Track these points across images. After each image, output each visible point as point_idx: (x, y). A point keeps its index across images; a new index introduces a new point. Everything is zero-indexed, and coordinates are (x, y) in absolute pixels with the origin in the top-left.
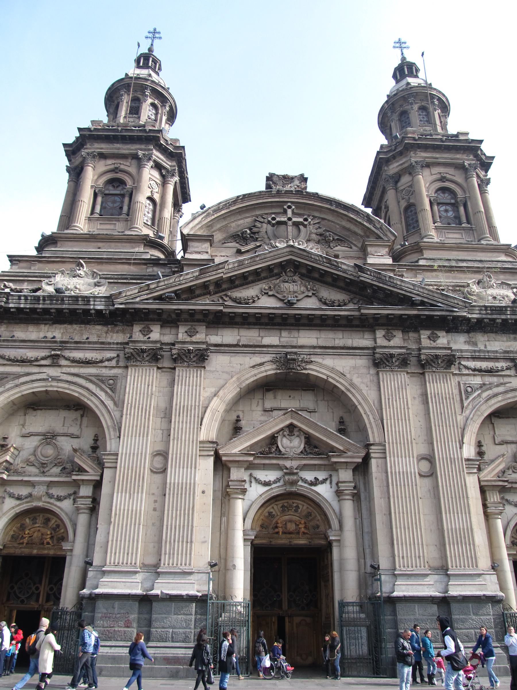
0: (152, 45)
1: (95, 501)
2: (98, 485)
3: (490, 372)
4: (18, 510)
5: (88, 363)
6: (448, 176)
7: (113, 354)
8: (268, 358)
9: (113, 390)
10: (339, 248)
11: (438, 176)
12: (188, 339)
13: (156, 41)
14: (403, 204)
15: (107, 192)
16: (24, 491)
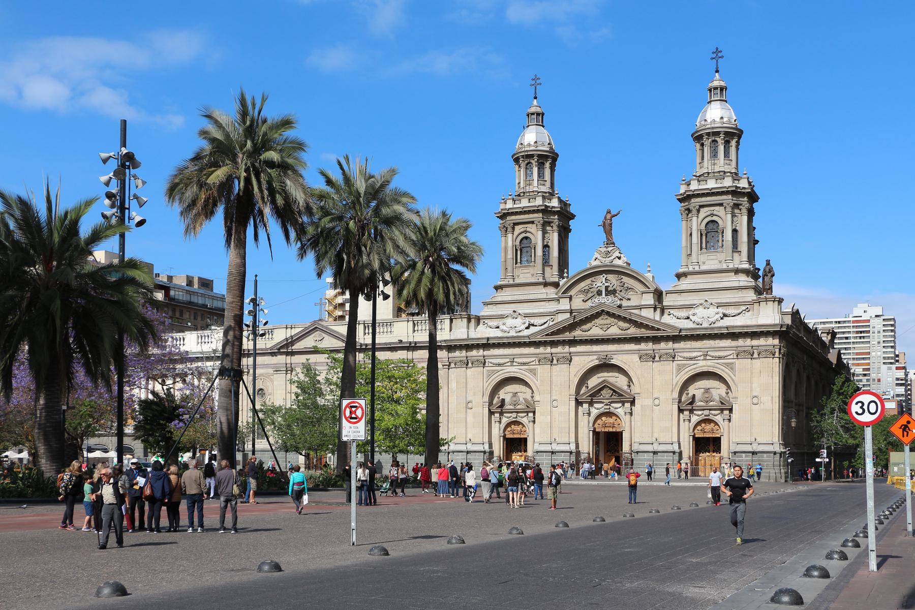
0: (535, 92)
1: (534, 418)
2: (534, 413)
3: (691, 359)
4: (508, 422)
5: (524, 364)
6: (715, 213)
7: (533, 359)
8: (595, 357)
9: (535, 374)
10: (631, 293)
11: (709, 213)
12: (563, 351)
13: (538, 87)
14: (689, 232)
15: (523, 246)
16: (509, 415)
